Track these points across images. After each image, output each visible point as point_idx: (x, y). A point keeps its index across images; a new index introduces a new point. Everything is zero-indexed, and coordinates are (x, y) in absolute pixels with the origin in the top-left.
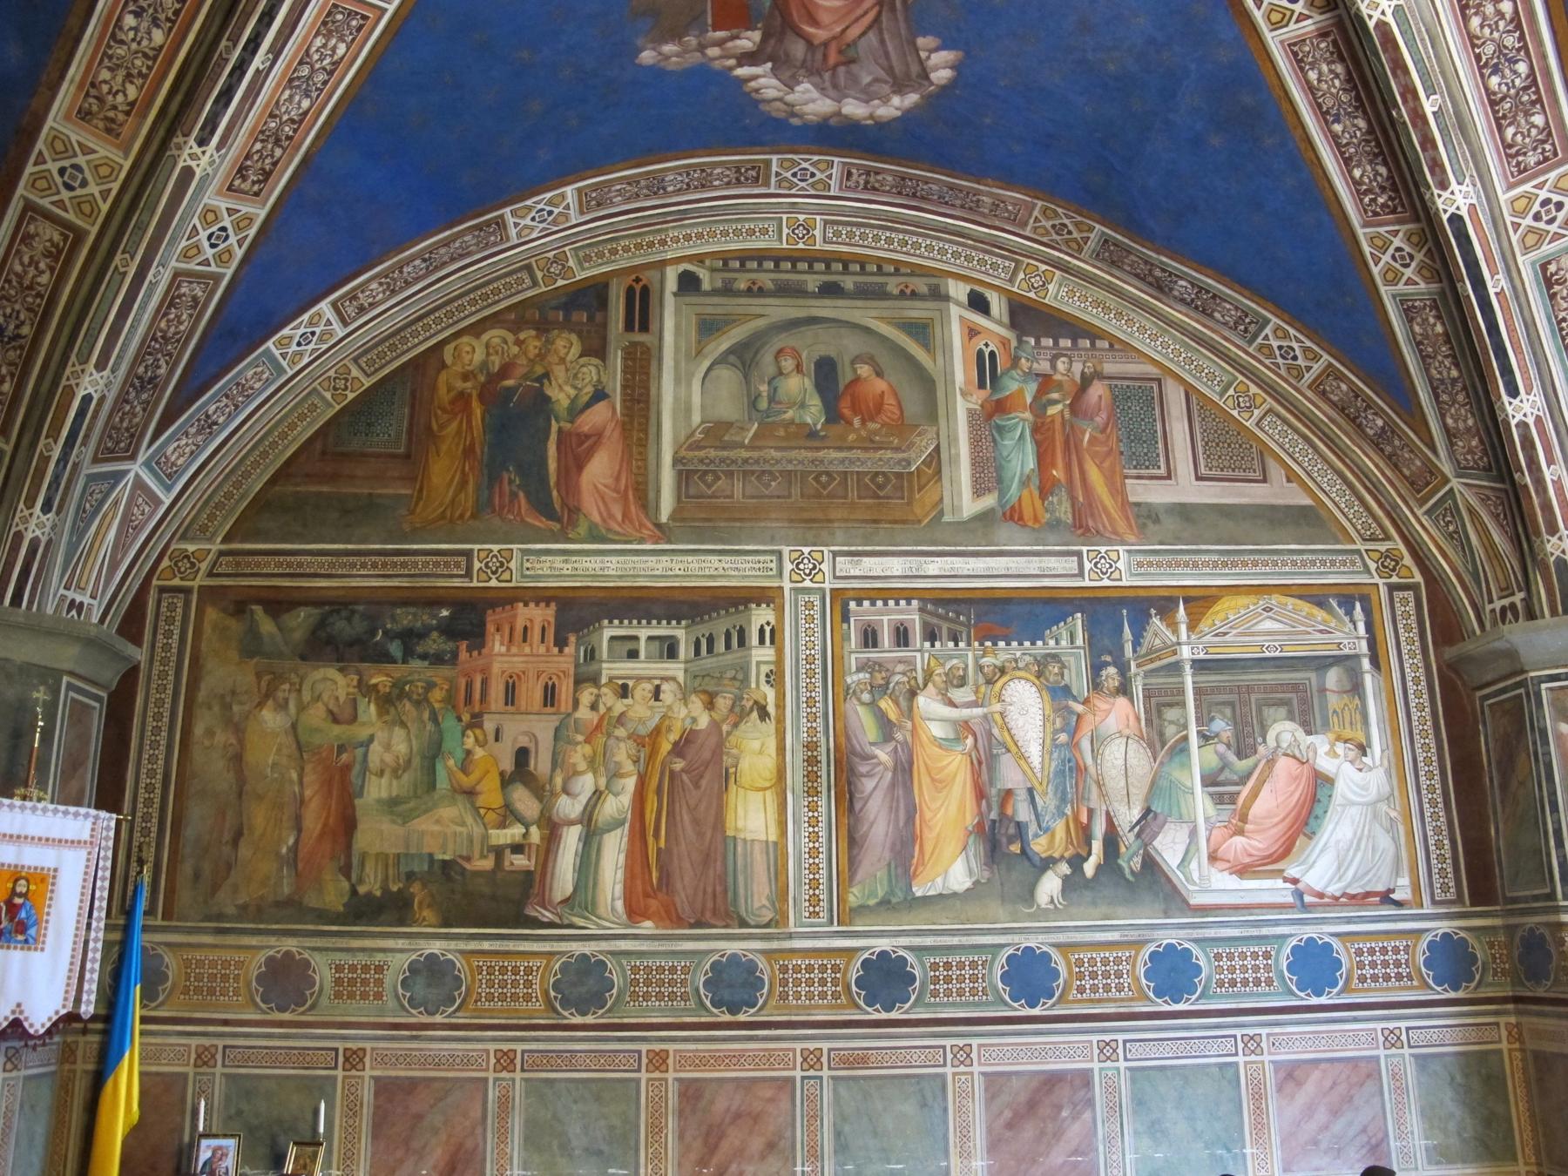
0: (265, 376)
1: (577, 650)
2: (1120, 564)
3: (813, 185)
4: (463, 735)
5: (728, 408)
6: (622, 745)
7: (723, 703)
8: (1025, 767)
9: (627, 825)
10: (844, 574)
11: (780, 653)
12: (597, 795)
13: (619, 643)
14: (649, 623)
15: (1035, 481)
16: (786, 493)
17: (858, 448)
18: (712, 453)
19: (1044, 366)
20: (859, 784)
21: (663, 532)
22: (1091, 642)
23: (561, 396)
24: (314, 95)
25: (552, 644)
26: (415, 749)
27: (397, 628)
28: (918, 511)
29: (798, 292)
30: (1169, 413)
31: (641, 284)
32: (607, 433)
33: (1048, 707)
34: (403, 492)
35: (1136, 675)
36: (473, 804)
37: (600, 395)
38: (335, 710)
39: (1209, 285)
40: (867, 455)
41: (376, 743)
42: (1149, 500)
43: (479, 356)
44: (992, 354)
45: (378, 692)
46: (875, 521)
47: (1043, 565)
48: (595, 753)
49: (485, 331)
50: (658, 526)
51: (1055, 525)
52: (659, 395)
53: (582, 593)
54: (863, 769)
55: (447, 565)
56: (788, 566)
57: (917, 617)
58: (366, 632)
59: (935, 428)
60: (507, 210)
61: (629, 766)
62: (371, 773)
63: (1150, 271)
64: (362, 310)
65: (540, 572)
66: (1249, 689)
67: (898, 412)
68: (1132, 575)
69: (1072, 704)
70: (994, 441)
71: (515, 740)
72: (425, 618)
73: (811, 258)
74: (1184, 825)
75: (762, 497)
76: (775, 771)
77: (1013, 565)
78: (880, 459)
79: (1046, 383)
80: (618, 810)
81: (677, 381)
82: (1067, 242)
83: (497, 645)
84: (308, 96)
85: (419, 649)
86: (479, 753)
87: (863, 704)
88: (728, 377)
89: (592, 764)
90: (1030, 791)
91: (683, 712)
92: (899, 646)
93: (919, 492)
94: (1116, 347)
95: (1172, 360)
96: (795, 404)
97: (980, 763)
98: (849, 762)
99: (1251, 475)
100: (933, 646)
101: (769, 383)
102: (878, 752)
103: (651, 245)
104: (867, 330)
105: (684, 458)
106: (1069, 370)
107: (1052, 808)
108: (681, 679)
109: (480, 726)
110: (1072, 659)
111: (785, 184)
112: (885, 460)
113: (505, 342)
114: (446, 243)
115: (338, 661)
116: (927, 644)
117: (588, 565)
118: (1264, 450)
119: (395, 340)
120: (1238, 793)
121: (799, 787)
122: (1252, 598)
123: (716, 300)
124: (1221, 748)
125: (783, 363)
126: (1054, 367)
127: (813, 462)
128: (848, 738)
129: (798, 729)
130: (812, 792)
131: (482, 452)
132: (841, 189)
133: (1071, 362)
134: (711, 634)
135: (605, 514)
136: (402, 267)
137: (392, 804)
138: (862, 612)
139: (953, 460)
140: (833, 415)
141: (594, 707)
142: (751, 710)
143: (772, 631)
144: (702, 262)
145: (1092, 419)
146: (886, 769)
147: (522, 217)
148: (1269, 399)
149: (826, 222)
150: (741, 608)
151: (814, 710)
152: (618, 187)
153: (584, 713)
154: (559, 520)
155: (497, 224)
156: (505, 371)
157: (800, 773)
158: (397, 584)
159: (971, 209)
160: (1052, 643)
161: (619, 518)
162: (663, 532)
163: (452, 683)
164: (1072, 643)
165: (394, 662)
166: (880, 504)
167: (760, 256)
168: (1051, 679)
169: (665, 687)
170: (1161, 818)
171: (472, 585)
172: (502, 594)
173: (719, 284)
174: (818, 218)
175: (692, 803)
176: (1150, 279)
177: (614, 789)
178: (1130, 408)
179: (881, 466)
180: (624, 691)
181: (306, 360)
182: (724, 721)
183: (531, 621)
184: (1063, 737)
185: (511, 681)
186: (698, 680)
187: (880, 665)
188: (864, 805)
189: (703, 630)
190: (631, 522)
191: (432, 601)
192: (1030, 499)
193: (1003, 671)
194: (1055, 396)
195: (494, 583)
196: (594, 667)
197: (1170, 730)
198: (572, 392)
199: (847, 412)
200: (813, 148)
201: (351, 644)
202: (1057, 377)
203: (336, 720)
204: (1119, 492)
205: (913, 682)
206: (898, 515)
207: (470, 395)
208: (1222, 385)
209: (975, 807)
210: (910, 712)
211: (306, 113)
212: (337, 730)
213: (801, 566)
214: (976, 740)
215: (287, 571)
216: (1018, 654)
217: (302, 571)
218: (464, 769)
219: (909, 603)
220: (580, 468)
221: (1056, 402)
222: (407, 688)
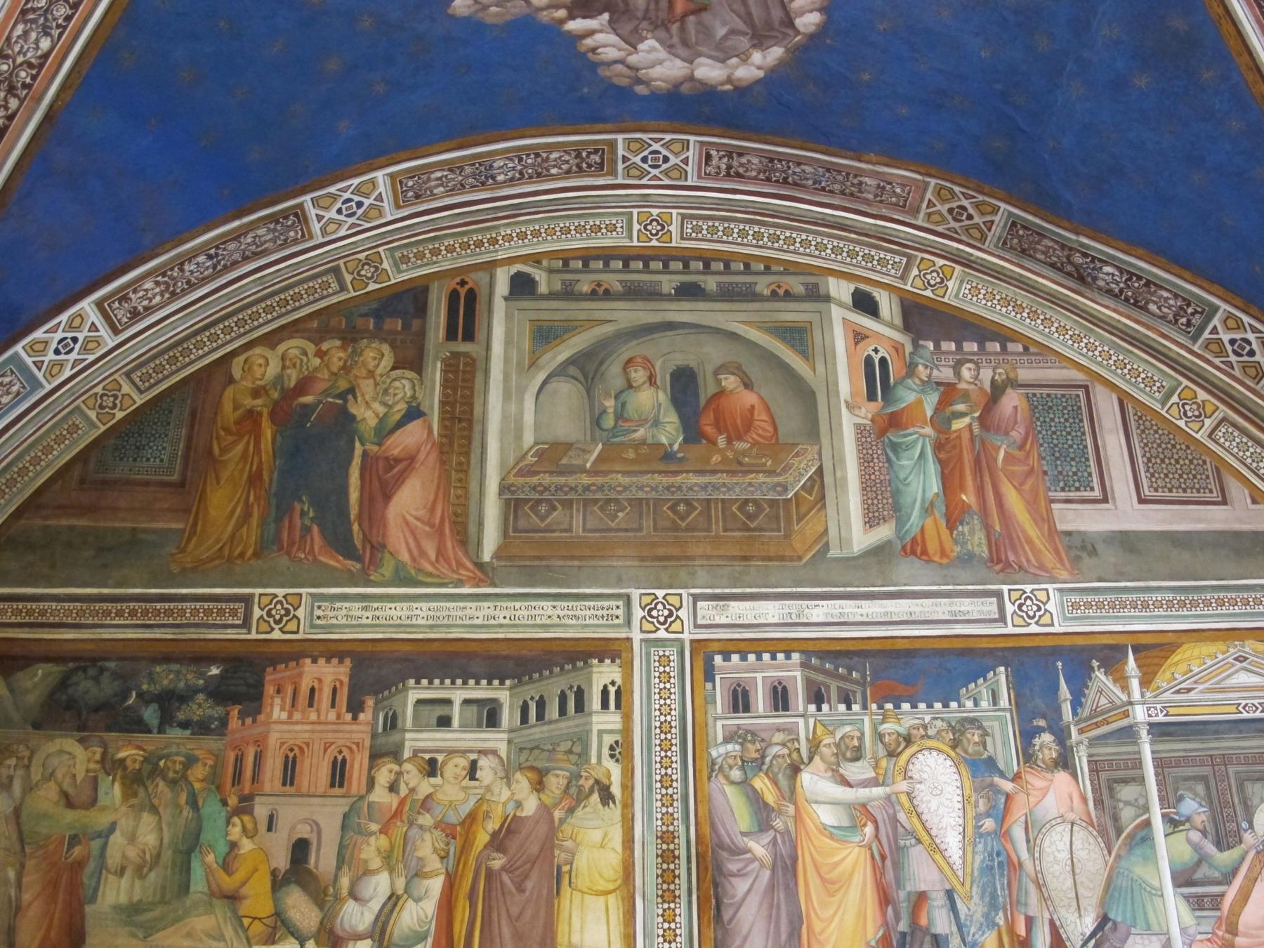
0: (15, 389)
1: (375, 718)
2: (1051, 606)
3: (666, 173)
4: (228, 822)
5: (567, 426)
6: (427, 836)
7: (555, 783)
8: (941, 862)
9: (430, 940)
10: (708, 622)
11: (628, 719)
12: (393, 900)
13: (428, 707)
14: (465, 683)
15: (940, 509)
16: (635, 526)
17: (723, 472)
18: (547, 479)
19: (946, 374)
20: (727, 884)
21: (484, 573)
22: (1020, 703)
23: (369, 414)
24: (56, 33)
25: (344, 709)
26: (166, 840)
27: (155, 689)
28: (797, 545)
29: (653, 294)
30: (1100, 426)
31: (467, 287)
32: (421, 456)
33: (967, 784)
34: (174, 526)
35: (1078, 744)
36: (235, 912)
37: (414, 413)
38: (71, 791)
39: (1141, 269)
40: (735, 480)
41: (118, 833)
42: (1082, 528)
43: (273, 369)
45: (125, 768)
46: (745, 558)
47: (954, 608)
48: (392, 847)
49: (281, 341)
50: (480, 565)
51: (967, 559)
52: (485, 412)
53: (385, 647)
54: (733, 867)
55: (221, 612)
56: (638, 613)
57: (798, 674)
58: (116, 695)
59: (816, 448)
60: (307, 199)
61: (434, 863)
62: (109, 871)
63: (1068, 257)
64: (135, 315)
65: (334, 621)
66: (1226, 760)
67: (770, 429)
68: (1066, 619)
69: (997, 780)
70: (889, 460)
71: (293, 828)
72: (189, 677)
73: (667, 257)
74: (1154, 938)
75: (610, 530)
76: (620, 869)
77: (917, 609)
78: (750, 484)
79: (949, 392)
80: (419, 920)
81: (507, 396)
82: (967, 230)
83: (276, 710)
84: (47, 34)
85: (181, 716)
86: (247, 845)
87: (732, 783)
88: (567, 391)
89: (388, 860)
90: (950, 894)
91: (506, 794)
92: (776, 709)
93: (799, 520)
94: (1032, 350)
95: (1100, 364)
96: (646, 421)
97: (883, 858)
98: (715, 858)
99: (1207, 496)
100: (819, 709)
101: (616, 397)
102: (752, 844)
103: (479, 244)
104: (734, 336)
105: (512, 485)
106: (976, 378)
107: (978, 916)
108: (504, 754)
109: (250, 811)
110: (996, 724)
111: (634, 172)
112: (758, 486)
113: (306, 354)
114: (237, 235)
115: (79, 729)
116: (812, 708)
117: (393, 612)
118: (1220, 467)
119: (176, 351)
120: (1222, 895)
121: (651, 890)
122: (1220, 646)
123: (554, 304)
124: (1195, 836)
125: (633, 375)
126: (958, 374)
127: (668, 488)
128: (713, 825)
129: (650, 814)
130: (668, 896)
131: (271, 480)
132: (699, 177)
133: (978, 369)
134: (542, 697)
135: (416, 553)
136: (182, 264)
137: (131, 913)
138: (729, 669)
139: (841, 484)
140: (692, 433)
141: (393, 788)
142: (591, 791)
143: (618, 693)
144: (539, 262)
145: (1007, 434)
146: (762, 865)
147: (327, 208)
148: (1222, 407)
149: (684, 217)
150: (580, 664)
151: (670, 791)
152: (439, 174)
153: (380, 795)
154: (359, 559)
155: (296, 215)
156: (303, 386)
157: (653, 872)
158: (158, 636)
159: (853, 195)
160: (969, 704)
161: (433, 555)
162: (486, 574)
163: (218, 758)
164: (995, 704)
165: (150, 732)
166: (750, 537)
167: (607, 255)
168: (970, 750)
169: (484, 762)
170: (1122, 928)
171: (249, 637)
172: (285, 648)
173: (558, 286)
174: (674, 212)
175: (515, 910)
176: (1069, 268)
177: (415, 894)
179: (752, 493)
180: (432, 768)
181: (68, 373)
182: (556, 805)
183: (320, 681)
184: (989, 824)
185: (291, 755)
186: (525, 754)
187: (753, 734)
188: (736, 913)
189: (531, 692)
190: (447, 561)
191: (199, 656)
192: (935, 528)
193: (908, 740)
194: (961, 407)
195: (277, 635)
196: (395, 737)
197: (1127, 813)
198: (381, 410)
199: (709, 430)
200: (664, 124)
201: (97, 710)
202: (963, 386)
203: (70, 804)
204: (1045, 520)
205: (795, 755)
206: (772, 551)
207: (260, 414)
209: (878, 914)
210: (792, 794)
211: (46, 56)
212: (70, 816)
213: (654, 613)
214: (877, 828)
215: (27, 620)
216: (928, 718)
217: (44, 620)
218: (226, 866)
219: (788, 657)
220: (387, 498)
221: (962, 415)
222: (162, 763)
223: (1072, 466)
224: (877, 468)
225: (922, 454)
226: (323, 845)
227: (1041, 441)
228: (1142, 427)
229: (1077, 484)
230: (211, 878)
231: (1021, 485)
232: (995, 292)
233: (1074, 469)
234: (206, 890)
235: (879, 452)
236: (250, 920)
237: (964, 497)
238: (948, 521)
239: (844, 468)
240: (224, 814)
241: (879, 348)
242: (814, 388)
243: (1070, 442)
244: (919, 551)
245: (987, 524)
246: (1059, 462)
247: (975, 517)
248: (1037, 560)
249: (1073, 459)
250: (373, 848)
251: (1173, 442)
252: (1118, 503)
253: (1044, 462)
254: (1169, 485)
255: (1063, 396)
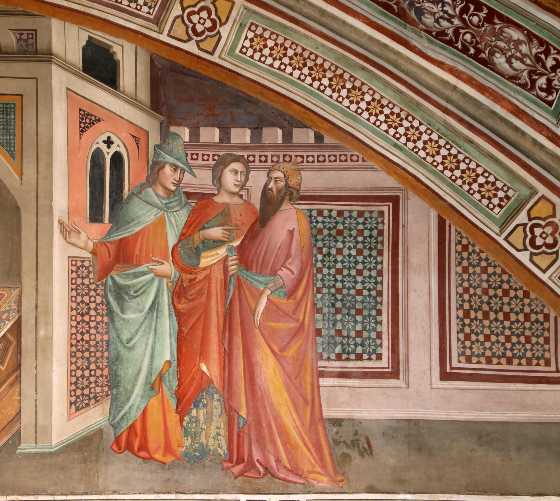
30: (406, 261)
42: (357, 415)
44: (117, 158)
59: (15, 293)
70: (110, 313)
94: (328, 140)
95: (421, 162)
106: (243, 186)
126: (218, 180)
133: (248, 170)
145: (274, 273)
178: (339, 251)
194: (216, 232)
202: (223, 199)
208: (507, 205)
221: (217, 243)
223: (356, 322)
224: (93, 324)
225: (155, 304)
227: (319, 284)
228: (465, 263)
229: (359, 350)
231: (282, 350)
232: (287, 44)
233: (359, 327)
235: (99, 299)
237: (204, 368)
238: (179, 402)
239: (49, 324)
241: (114, 138)
242: (20, 204)
243: (359, 286)
244: (136, 447)
245: (230, 407)
246: (339, 317)
247: (216, 396)
248: (289, 461)
249: (359, 312)
251: (505, 286)
252: (411, 379)
253: (319, 316)
254: (488, 353)
255: (361, 214)
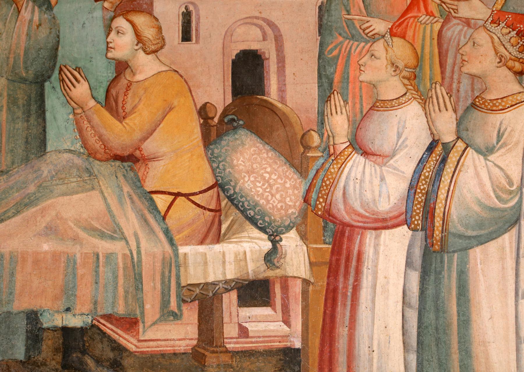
4: (108, 30)
6: (482, 37)
48: (419, 59)
226: (287, 61)
230: (86, 125)
234: (78, 146)
236: (171, 198)
240: (98, 13)
250: (382, 62)
